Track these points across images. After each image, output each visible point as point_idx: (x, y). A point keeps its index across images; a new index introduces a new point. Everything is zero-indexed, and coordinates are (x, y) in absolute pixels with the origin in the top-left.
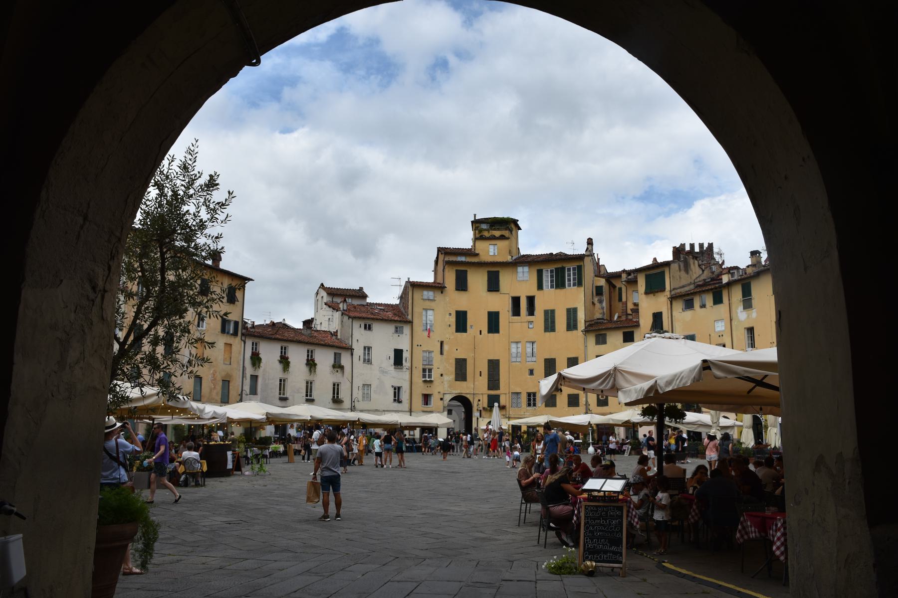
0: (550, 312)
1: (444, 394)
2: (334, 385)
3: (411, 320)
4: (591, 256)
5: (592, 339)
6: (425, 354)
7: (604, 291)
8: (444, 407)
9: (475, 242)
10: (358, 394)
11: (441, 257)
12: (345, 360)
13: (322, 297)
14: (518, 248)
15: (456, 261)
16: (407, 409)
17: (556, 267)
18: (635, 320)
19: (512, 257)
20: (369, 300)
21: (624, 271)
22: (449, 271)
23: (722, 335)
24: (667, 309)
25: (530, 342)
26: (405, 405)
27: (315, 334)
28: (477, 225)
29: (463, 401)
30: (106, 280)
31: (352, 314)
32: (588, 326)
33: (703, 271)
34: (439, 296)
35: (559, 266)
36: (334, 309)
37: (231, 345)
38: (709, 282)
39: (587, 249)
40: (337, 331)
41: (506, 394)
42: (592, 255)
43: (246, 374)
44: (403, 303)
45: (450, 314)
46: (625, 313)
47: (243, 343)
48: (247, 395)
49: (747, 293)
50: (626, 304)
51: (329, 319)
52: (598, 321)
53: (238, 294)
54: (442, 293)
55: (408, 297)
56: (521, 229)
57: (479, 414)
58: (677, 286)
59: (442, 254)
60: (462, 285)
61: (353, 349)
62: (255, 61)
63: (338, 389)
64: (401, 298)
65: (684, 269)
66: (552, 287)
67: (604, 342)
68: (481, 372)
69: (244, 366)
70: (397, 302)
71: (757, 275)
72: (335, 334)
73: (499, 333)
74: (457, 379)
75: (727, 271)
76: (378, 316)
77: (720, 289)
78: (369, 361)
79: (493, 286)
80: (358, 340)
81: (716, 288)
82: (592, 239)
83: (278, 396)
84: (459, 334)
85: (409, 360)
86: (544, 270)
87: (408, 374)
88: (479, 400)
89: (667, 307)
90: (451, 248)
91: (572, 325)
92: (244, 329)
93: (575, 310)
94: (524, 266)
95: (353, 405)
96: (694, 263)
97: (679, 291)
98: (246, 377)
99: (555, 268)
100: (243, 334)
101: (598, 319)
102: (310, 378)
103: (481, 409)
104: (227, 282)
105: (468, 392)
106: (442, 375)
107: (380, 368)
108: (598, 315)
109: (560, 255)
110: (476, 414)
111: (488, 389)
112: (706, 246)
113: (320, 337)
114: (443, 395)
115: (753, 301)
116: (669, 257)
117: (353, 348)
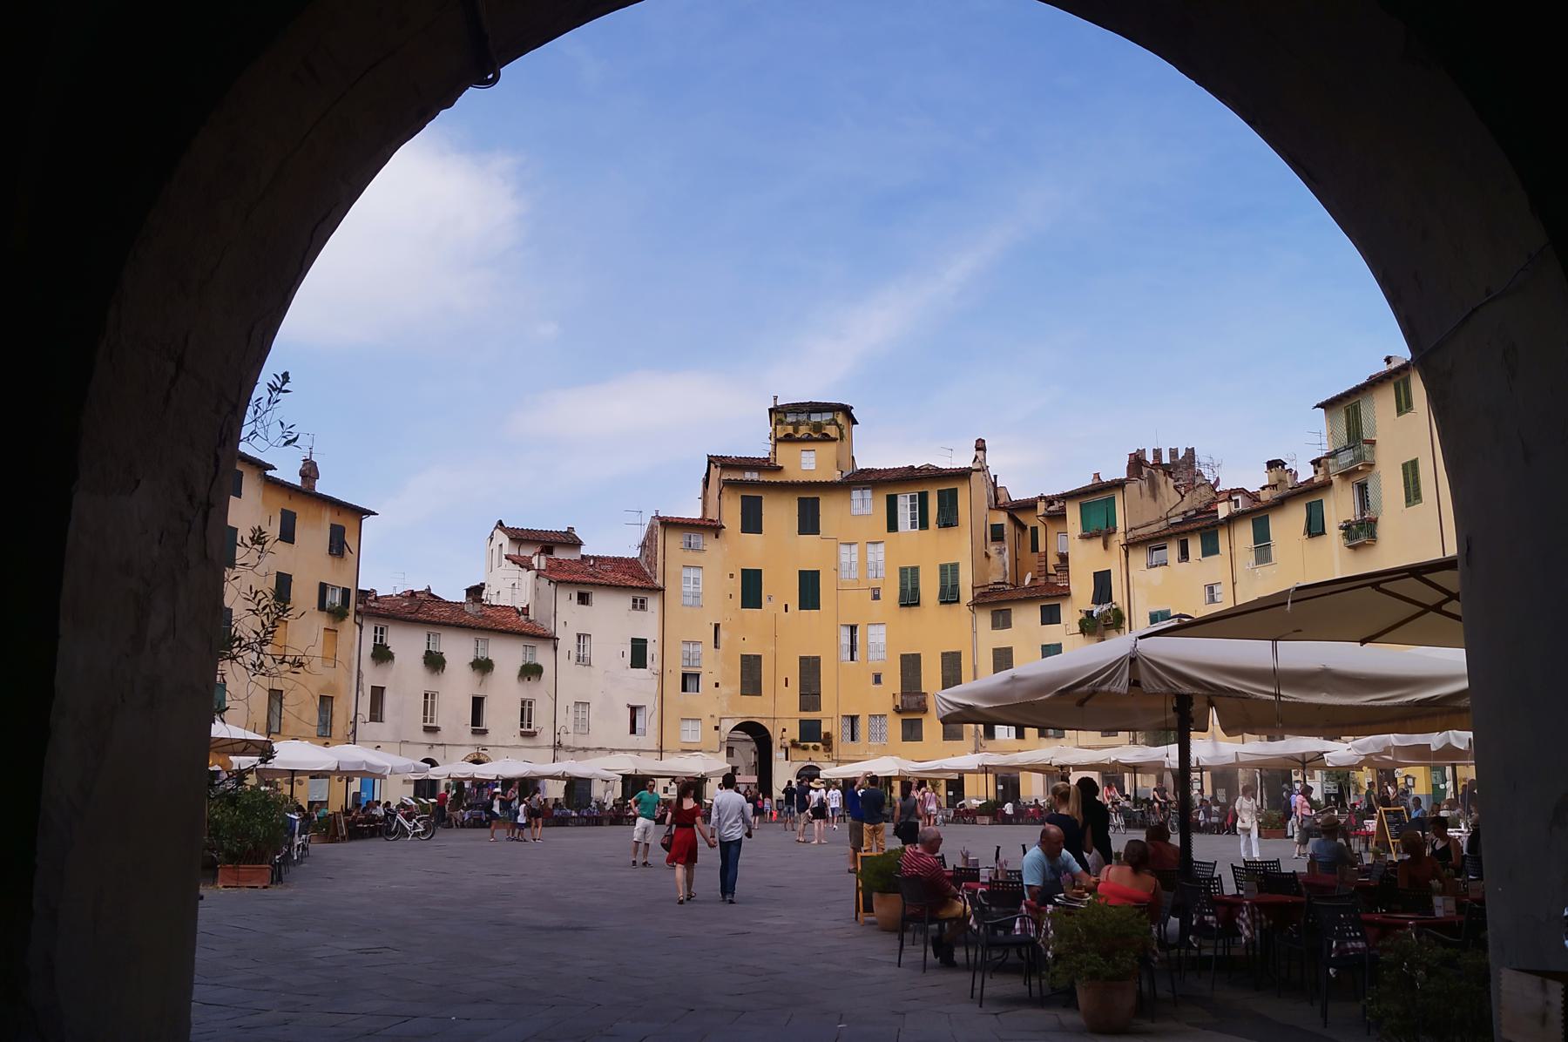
0: (909, 571)
1: (721, 718)
2: (523, 703)
3: (662, 586)
4: (984, 470)
5: (985, 619)
6: (686, 648)
7: (1005, 533)
8: (721, 742)
9: (776, 445)
10: (566, 720)
11: (715, 473)
12: (543, 656)
13: (501, 545)
14: (853, 457)
15: (741, 480)
16: (655, 748)
18: (1061, 585)
19: (842, 472)
20: (584, 551)
21: (1041, 498)
22: (729, 498)
26: (649, 739)
27: (489, 612)
28: (780, 416)
29: (756, 733)
30: (212, 484)
31: (554, 576)
32: (978, 595)
33: (1183, 496)
34: (709, 543)
36: (521, 566)
37: (337, 631)
38: (1193, 516)
39: (976, 457)
40: (528, 606)
41: (832, 718)
42: (984, 469)
43: (363, 684)
44: (647, 556)
46: (1044, 572)
47: (357, 627)
48: (365, 722)
49: (1262, 537)
51: (514, 584)
52: (995, 587)
53: (350, 540)
54: (717, 537)
55: (656, 545)
56: (857, 423)
58: (1137, 524)
59: (716, 467)
60: (752, 522)
61: (558, 639)
62: (490, 76)
63: (530, 710)
64: (643, 546)
65: (1149, 493)
66: (913, 526)
67: (1007, 625)
68: (786, 679)
69: (359, 670)
70: (636, 554)
71: (1280, 503)
72: (525, 611)
75: (1227, 496)
76: (602, 578)
77: (1215, 529)
78: (587, 662)
79: (809, 523)
80: (565, 622)
81: (1207, 528)
82: (984, 441)
83: (421, 724)
85: (658, 658)
90: (733, 456)
91: (949, 596)
92: (360, 603)
93: (955, 567)
94: (864, 489)
95: (557, 740)
96: (1166, 482)
97: (1140, 532)
98: (363, 690)
99: (919, 493)
100: (357, 612)
101: (995, 583)
102: (479, 694)
103: (789, 744)
104: (328, 518)
105: (763, 715)
106: (717, 685)
107: (606, 672)
108: (996, 577)
109: (927, 469)
110: (778, 755)
112: (1181, 454)
113: (497, 615)
116: (1122, 474)
117: (557, 636)
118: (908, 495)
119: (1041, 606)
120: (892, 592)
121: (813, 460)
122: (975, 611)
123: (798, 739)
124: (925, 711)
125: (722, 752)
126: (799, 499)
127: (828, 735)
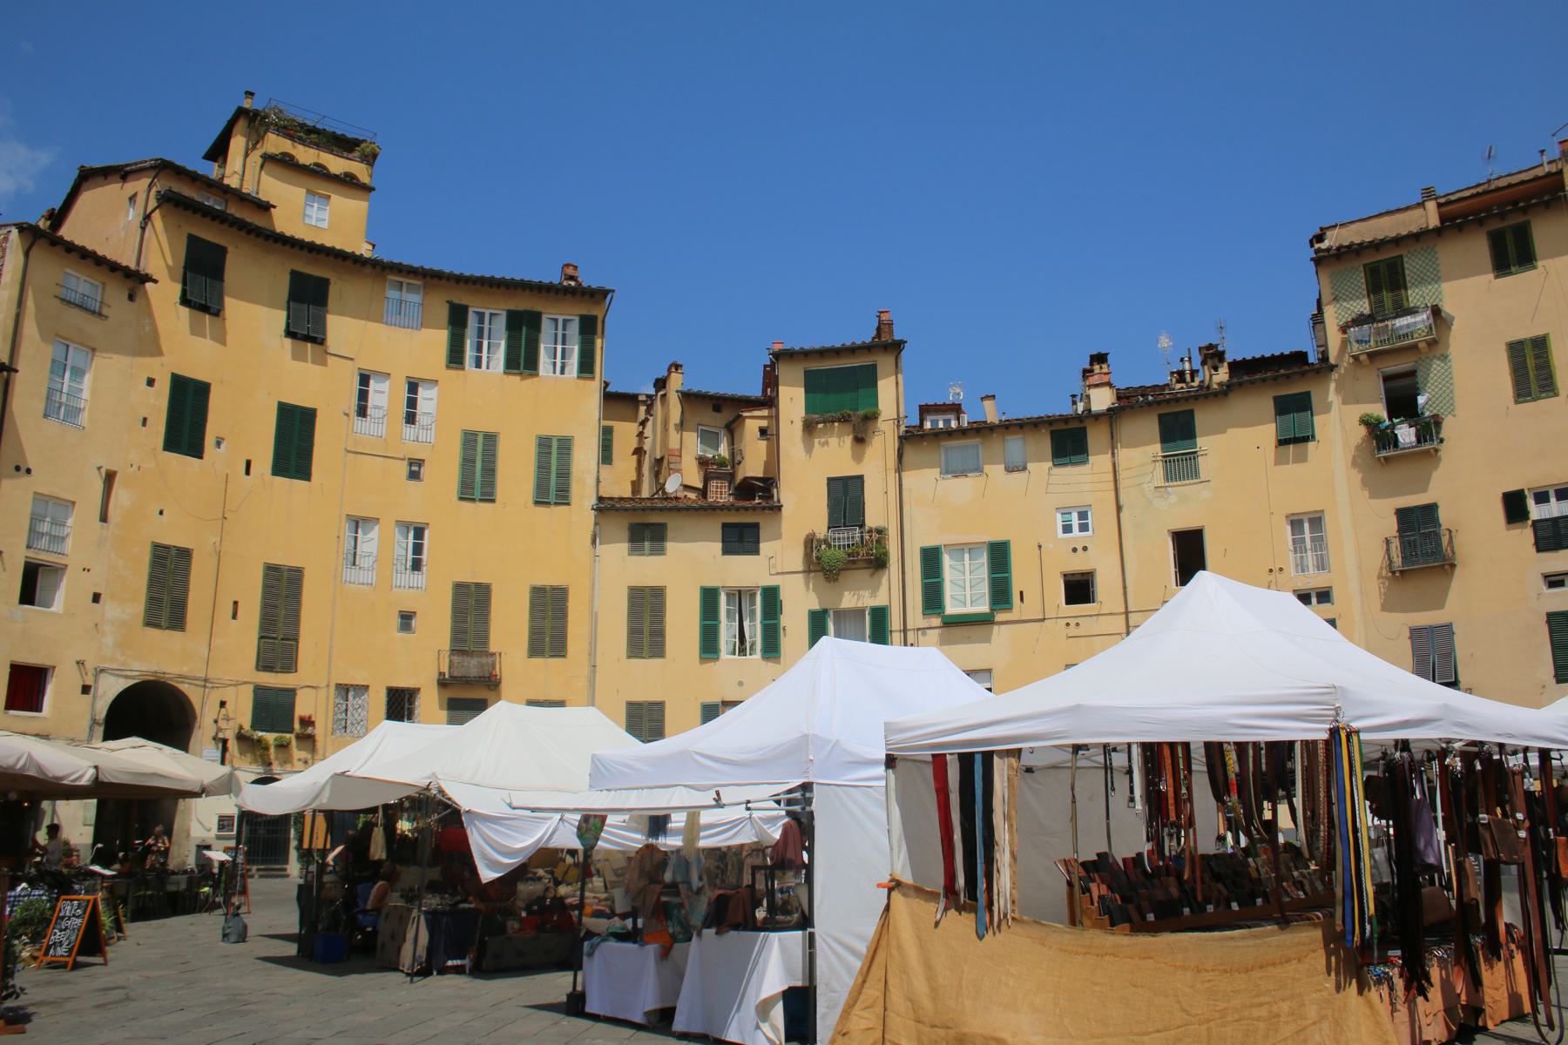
0: (480, 439)
8: (94, 722)
17: (512, 307)
23: (1085, 549)
35: (523, 304)
45: (151, 382)
50: (681, 457)
54: (131, 297)
57: (218, 754)
67: (660, 551)
68: (236, 603)
73: (309, 479)
82: (576, 268)
84: (175, 459)
86: (471, 310)
88: (223, 704)
93: (566, 445)
103: (230, 735)
105: (185, 670)
106: (96, 598)
111: (258, 669)
114: (96, 677)
119: (725, 526)
120: (445, 472)
121: (326, 215)
123: (246, 720)
126: (296, 277)
127: (307, 722)
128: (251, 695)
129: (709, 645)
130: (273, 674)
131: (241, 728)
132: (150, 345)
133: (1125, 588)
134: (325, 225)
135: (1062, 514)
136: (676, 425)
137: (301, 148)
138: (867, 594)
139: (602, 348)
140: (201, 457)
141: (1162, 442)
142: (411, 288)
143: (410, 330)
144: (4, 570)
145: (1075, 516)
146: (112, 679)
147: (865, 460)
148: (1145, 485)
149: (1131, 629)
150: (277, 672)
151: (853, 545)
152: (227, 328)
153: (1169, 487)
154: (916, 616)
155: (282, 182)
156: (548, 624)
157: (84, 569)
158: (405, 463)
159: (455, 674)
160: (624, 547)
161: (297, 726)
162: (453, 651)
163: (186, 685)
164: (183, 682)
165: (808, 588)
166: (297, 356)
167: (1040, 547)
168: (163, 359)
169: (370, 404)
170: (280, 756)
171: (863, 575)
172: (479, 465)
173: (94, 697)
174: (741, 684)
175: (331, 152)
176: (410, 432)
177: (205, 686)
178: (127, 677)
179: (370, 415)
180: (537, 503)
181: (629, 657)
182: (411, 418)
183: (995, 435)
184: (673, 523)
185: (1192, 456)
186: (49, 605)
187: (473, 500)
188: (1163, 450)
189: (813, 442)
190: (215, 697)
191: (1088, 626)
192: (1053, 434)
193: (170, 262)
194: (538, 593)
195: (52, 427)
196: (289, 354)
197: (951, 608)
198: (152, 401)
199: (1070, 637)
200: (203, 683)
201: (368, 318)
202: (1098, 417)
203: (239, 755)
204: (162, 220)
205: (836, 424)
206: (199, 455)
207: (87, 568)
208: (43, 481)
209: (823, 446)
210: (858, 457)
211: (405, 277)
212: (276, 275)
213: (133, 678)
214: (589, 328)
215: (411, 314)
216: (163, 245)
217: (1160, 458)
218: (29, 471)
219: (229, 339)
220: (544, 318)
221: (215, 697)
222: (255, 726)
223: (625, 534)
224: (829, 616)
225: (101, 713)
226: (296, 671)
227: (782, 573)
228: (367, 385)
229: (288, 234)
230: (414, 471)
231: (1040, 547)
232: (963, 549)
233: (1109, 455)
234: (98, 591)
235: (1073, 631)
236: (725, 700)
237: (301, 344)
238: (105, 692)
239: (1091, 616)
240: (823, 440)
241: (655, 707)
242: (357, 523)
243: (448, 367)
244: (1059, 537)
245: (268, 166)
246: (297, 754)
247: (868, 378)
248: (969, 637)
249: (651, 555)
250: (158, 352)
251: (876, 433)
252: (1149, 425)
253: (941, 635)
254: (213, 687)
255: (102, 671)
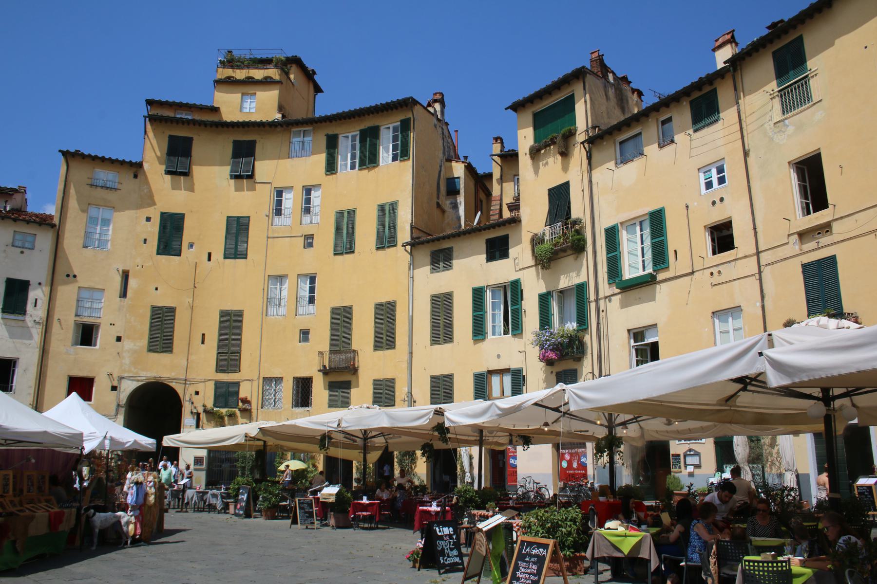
0: (346, 214)
1: (121, 378)
8: (119, 405)
17: (362, 127)
23: (722, 200)
24: (579, 173)
25: (306, 275)
45: (148, 219)
46: (497, 217)
50: (501, 200)
54: (136, 176)
56: (322, 92)
57: (194, 422)
65: (615, 100)
66: (353, 167)
67: (449, 267)
68: (203, 335)
73: (246, 258)
74: (152, 348)
82: (441, 94)
84: (164, 258)
87: (37, 334)
89: (579, 168)
93: (393, 206)
106: (119, 339)
111: (217, 371)
115: (813, 83)
118: (350, 135)
120: (326, 239)
122: (415, 253)
124: (355, 371)
125: (119, 416)
127: (245, 401)
128: (213, 386)
129: (479, 331)
130: (226, 374)
131: (204, 406)
132: (148, 200)
133: (755, 229)
134: (253, 110)
135: (705, 173)
136: (497, 180)
137: (238, 71)
138: (574, 274)
139: (413, 138)
140: (179, 255)
141: (776, 79)
142: (305, 134)
143: (305, 158)
144: (62, 329)
145: (714, 171)
146: (129, 382)
147: (570, 168)
148: (765, 126)
149: (762, 268)
150: (228, 373)
151: (555, 238)
152: (195, 181)
153: (787, 119)
154: (605, 289)
155: (227, 93)
156: (384, 328)
157: (111, 324)
158: (303, 238)
159: (333, 366)
160: (428, 268)
161: (240, 404)
162: (331, 352)
163: (174, 384)
164: (172, 382)
165: (538, 275)
166: (237, 189)
167: (687, 207)
168: (156, 206)
169: (283, 208)
170: (231, 422)
171: (569, 260)
172: (345, 231)
173: (120, 392)
174: (499, 356)
175: (256, 68)
176: (306, 219)
177: (185, 384)
178: (138, 381)
179: (284, 214)
180: (378, 249)
181: (432, 344)
182: (307, 210)
183: (650, 120)
184: (457, 246)
185: (803, 81)
186: (95, 345)
187: (342, 254)
188: (779, 85)
189: (539, 165)
190: (191, 390)
191: (729, 272)
192: (691, 103)
193: (159, 154)
194: (378, 306)
195: (88, 252)
196: (233, 188)
197: (628, 274)
198: (149, 229)
199: (714, 285)
200: (184, 382)
201: (279, 158)
202: (720, 74)
203: (207, 423)
204: (154, 132)
205: (552, 147)
206: (179, 254)
207: (113, 323)
208: (82, 281)
209: (545, 166)
210: (565, 168)
211: (301, 127)
212: (225, 145)
213: (142, 381)
214: (405, 126)
215: (308, 149)
216: (154, 145)
217: (777, 94)
218: (75, 276)
219: (196, 187)
220: (382, 128)
221: (191, 390)
222: (215, 405)
223: (428, 259)
224: (553, 296)
225: (122, 401)
226: (240, 371)
227: (523, 269)
228: (281, 196)
229: (235, 121)
230: (310, 242)
231: (687, 207)
232: (635, 224)
233: (735, 107)
234: (119, 335)
235: (716, 279)
236: (490, 369)
237: (240, 181)
238: (125, 389)
239: (729, 262)
240: (545, 162)
241: (448, 379)
242: (280, 278)
243: (327, 175)
244: (702, 194)
245: (219, 87)
246: (240, 420)
247: (569, 105)
248: (640, 298)
249: (443, 271)
250: (154, 204)
251: (576, 146)
252: (766, 66)
253: (621, 300)
254: (190, 384)
255: (123, 378)
